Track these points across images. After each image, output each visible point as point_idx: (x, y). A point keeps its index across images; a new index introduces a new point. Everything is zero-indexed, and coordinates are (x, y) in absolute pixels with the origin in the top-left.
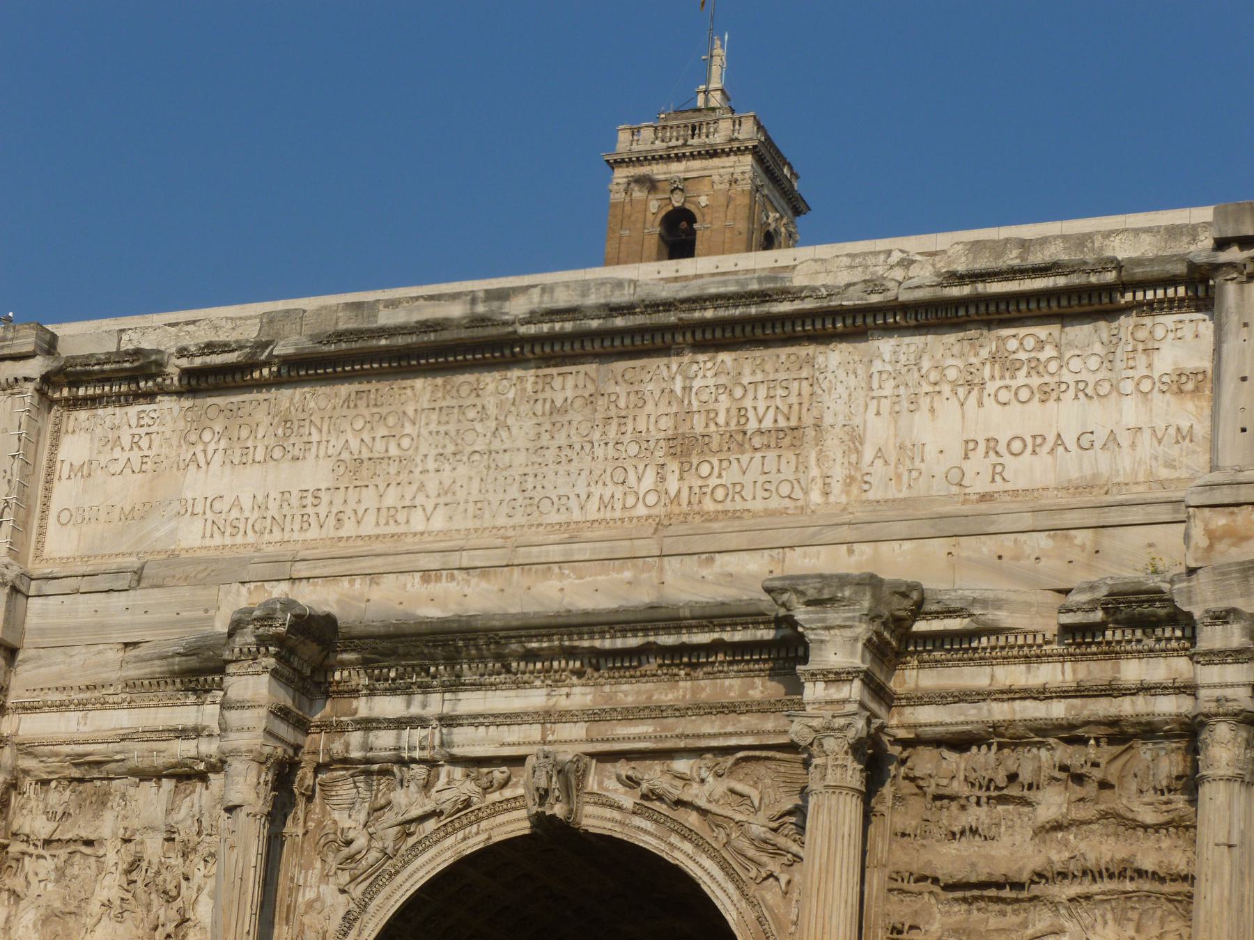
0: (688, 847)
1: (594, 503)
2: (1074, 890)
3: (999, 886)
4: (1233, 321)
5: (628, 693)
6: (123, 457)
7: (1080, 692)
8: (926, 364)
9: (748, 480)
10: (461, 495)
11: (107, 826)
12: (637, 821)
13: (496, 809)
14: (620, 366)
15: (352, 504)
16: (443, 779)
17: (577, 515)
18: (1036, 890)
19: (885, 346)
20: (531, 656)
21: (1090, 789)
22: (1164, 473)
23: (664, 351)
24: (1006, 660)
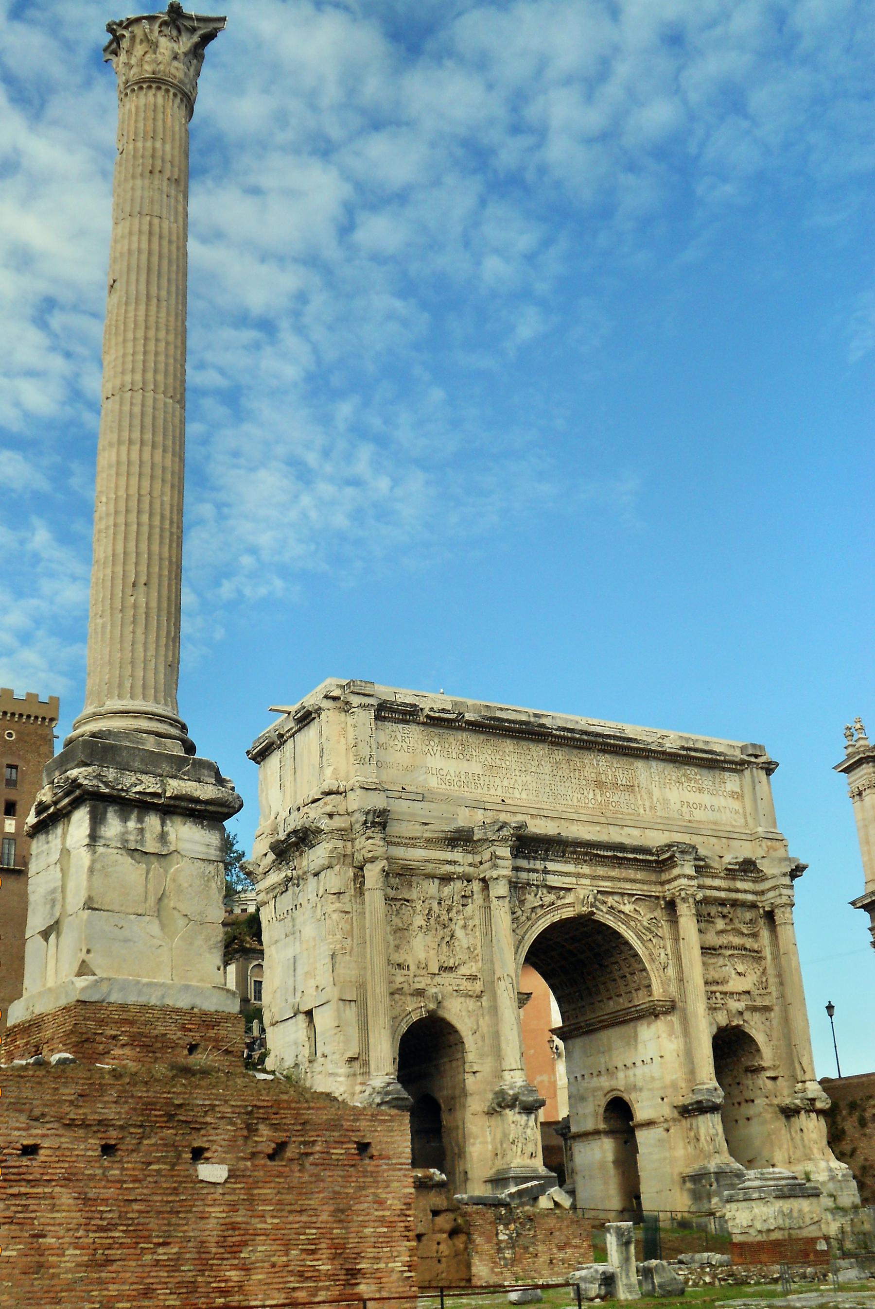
0: (624, 927)
1: (575, 800)
2: (730, 952)
3: (710, 949)
4: (756, 781)
5: (601, 871)
6: (400, 744)
7: (729, 890)
8: (666, 773)
9: (622, 800)
10: (530, 787)
11: (414, 894)
12: (607, 916)
13: (565, 906)
14: (575, 751)
15: (492, 781)
16: (540, 893)
17: (570, 803)
18: (720, 952)
19: (654, 764)
20: (575, 852)
21: (727, 921)
22: (734, 823)
23: (589, 749)
24: (707, 877)
